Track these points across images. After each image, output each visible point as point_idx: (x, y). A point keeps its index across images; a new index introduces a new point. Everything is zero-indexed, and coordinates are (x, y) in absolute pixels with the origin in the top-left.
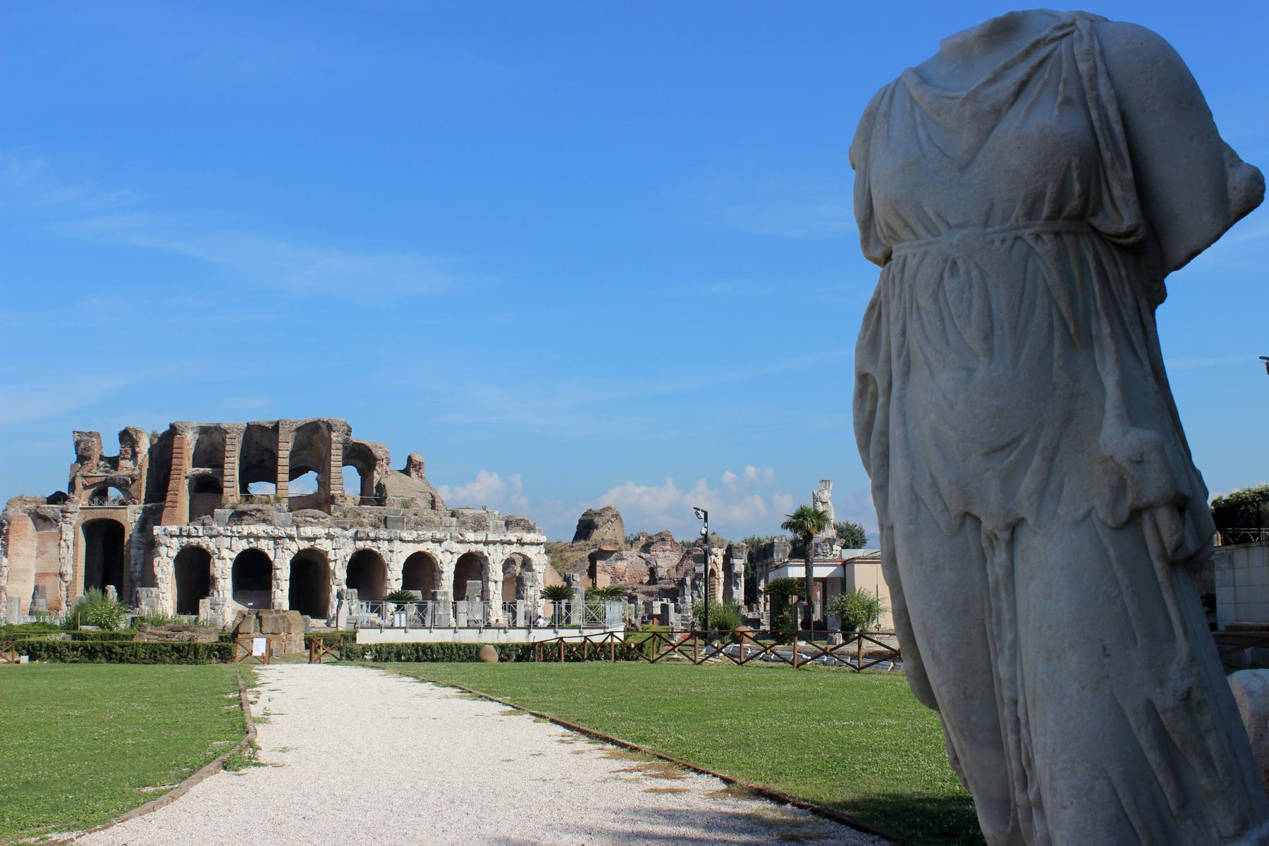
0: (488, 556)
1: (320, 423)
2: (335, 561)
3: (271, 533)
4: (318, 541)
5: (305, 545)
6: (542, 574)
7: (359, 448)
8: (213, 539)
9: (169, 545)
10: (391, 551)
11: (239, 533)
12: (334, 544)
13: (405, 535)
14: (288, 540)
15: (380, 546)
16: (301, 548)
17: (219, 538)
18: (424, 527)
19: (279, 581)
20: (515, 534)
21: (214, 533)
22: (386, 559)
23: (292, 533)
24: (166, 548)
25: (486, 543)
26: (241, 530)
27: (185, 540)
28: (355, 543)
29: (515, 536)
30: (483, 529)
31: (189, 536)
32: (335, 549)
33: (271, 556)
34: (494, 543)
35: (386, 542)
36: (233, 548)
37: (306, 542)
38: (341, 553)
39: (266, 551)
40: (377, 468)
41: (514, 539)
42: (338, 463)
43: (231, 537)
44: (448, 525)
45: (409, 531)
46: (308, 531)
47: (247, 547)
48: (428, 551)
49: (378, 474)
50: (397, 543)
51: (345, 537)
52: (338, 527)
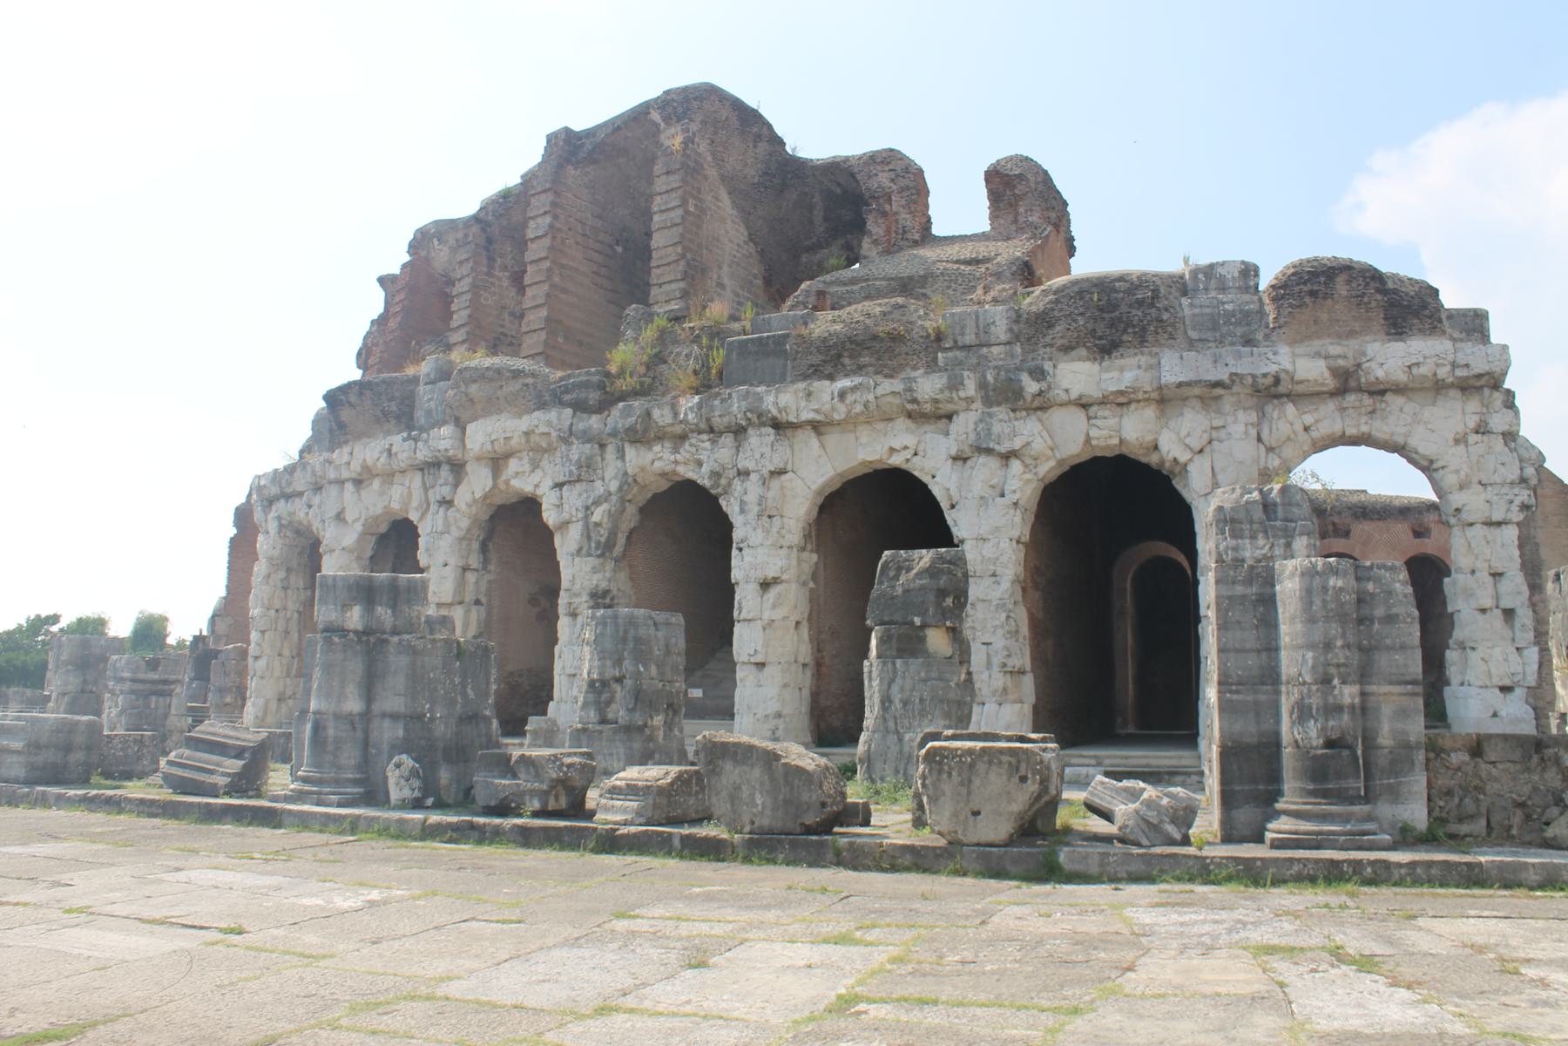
0: (1183, 457)
2: (564, 525)
6: (1512, 533)
7: (839, 184)
10: (744, 474)
13: (787, 400)
14: (445, 472)
15: (703, 457)
18: (865, 360)
20: (1317, 344)
22: (730, 506)
23: (443, 445)
25: (1166, 400)
29: (1318, 355)
30: (1142, 341)
31: (288, 497)
34: (1210, 393)
35: (728, 439)
36: (349, 517)
38: (574, 498)
40: (870, 225)
41: (1311, 368)
42: (672, 214)
43: (342, 482)
44: (969, 338)
45: (801, 385)
46: (480, 434)
49: (875, 242)
50: (759, 443)
51: (587, 437)
52: (562, 404)
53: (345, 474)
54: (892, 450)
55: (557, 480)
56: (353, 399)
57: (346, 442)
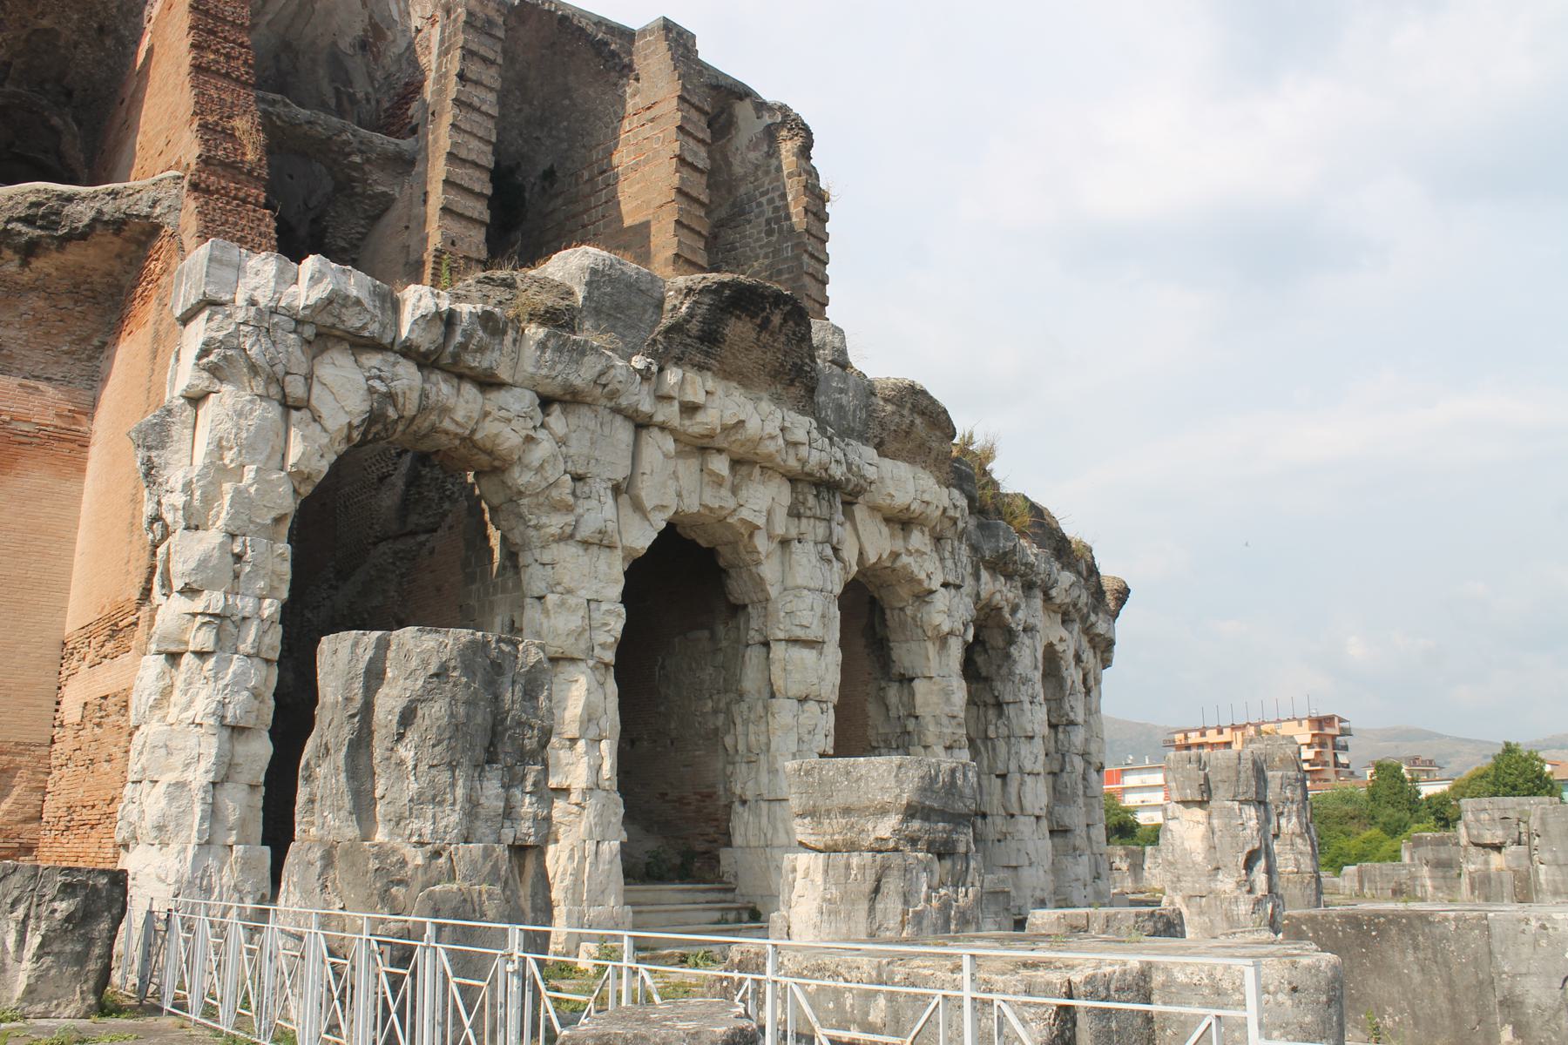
1: (743, 110)
3: (803, 451)
4: (919, 540)
5: (877, 543)
8: (556, 409)
9: (296, 388)
11: (690, 409)
12: (949, 563)
16: (872, 558)
17: (584, 418)
19: (812, 706)
21: (582, 375)
24: (274, 412)
26: (700, 398)
27: (407, 376)
28: (977, 577)
32: (945, 585)
33: (769, 571)
36: (649, 492)
37: (885, 530)
39: (761, 543)
43: (641, 424)
47: (692, 505)
48: (1060, 647)
52: (962, 490)
53: (668, 413)
54: (1061, 640)
55: (951, 579)
56: (777, 320)
57: (701, 368)
